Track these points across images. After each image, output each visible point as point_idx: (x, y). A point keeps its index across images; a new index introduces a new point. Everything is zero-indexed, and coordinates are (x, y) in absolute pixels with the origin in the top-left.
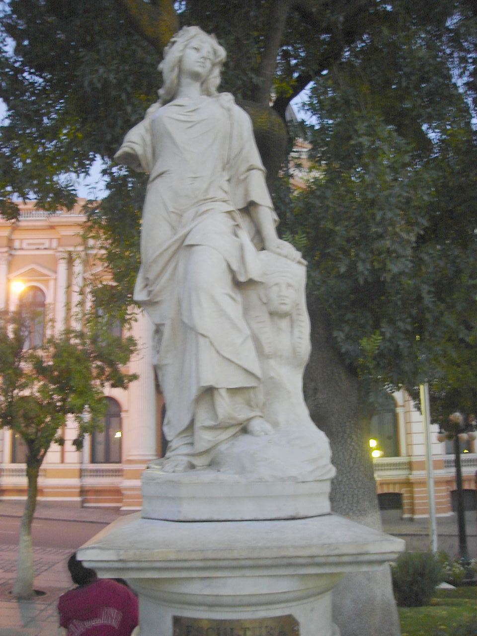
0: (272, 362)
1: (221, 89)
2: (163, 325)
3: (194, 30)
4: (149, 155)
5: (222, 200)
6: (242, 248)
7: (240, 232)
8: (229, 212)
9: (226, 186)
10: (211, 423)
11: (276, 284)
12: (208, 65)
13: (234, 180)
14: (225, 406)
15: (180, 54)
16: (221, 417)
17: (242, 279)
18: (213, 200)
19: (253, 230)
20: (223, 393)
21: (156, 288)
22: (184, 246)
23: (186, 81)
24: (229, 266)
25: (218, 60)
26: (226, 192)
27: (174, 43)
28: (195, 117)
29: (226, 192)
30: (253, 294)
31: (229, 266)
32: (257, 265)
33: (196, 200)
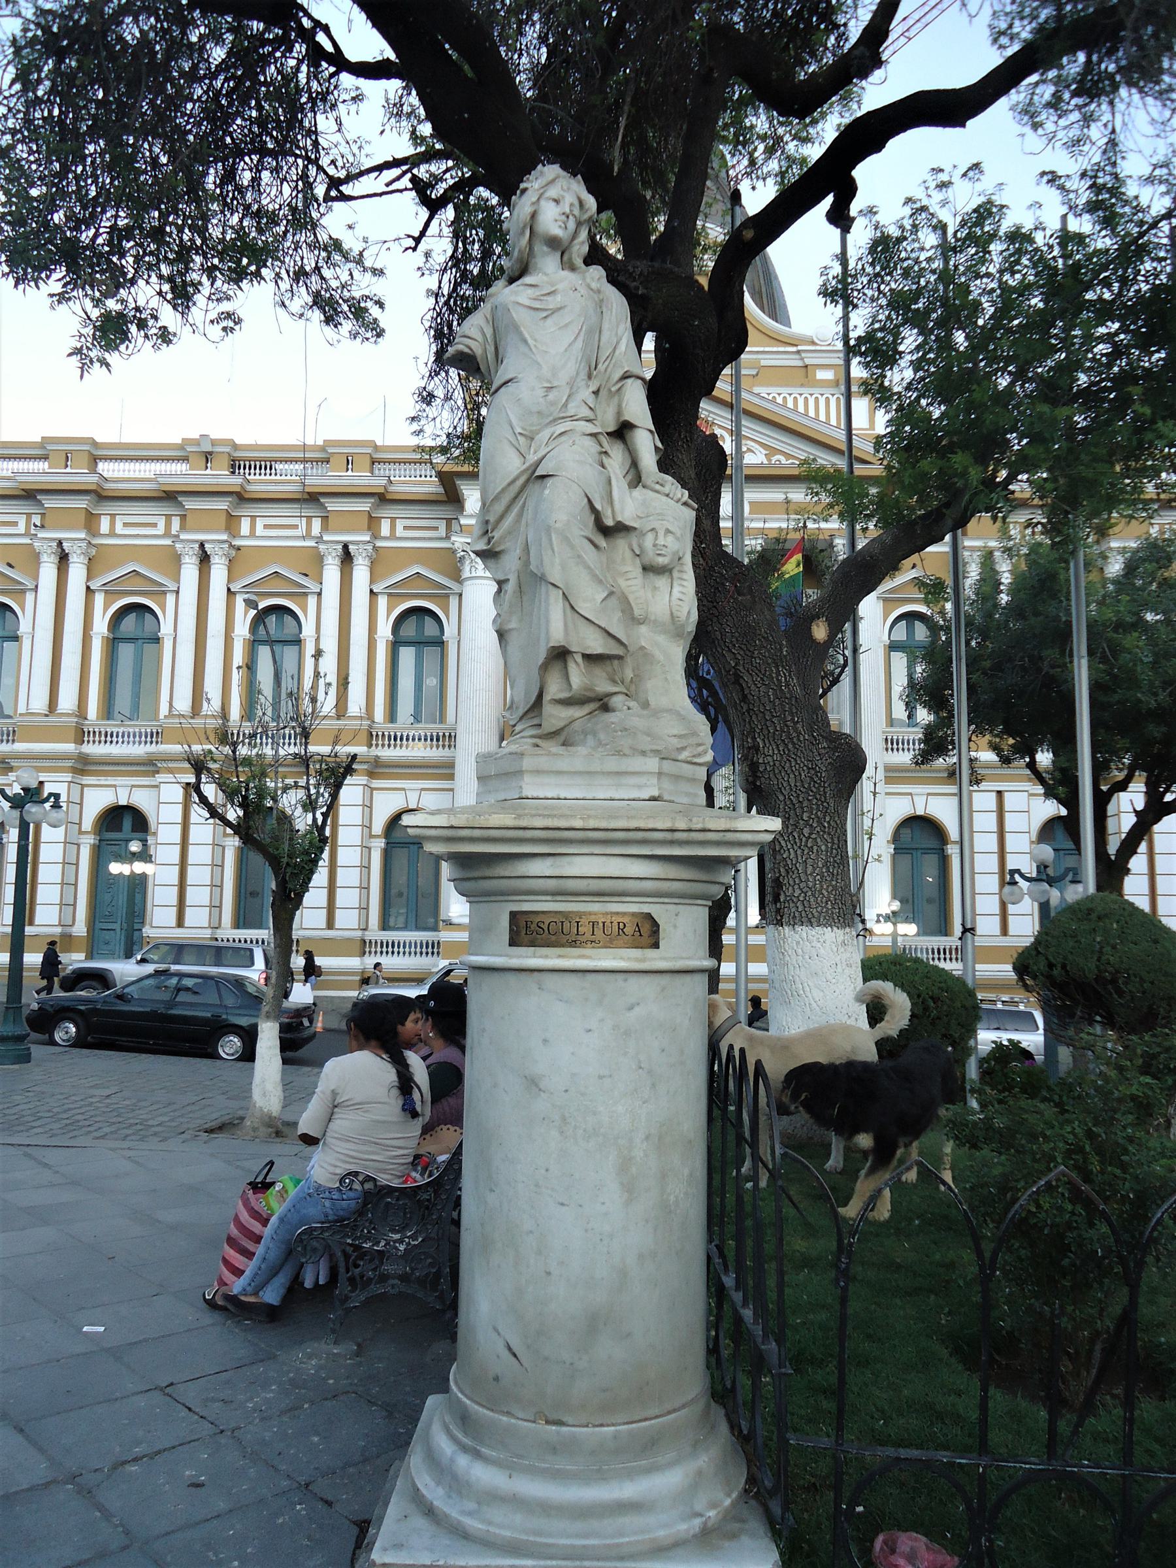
0: (643, 629)
1: (588, 262)
2: (508, 580)
3: (551, 171)
4: (491, 356)
7: (606, 460)
8: (594, 435)
9: (591, 401)
10: (564, 695)
11: (653, 529)
12: (572, 225)
13: (603, 393)
14: (578, 676)
16: (575, 686)
17: (609, 522)
18: (573, 418)
19: (630, 462)
20: (579, 659)
21: (497, 534)
22: (536, 477)
23: (540, 248)
24: (589, 501)
25: (586, 216)
27: (524, 191)
28: (552, 303)
30: (621, 544)
31: (589, 501)
32: (627, 506)
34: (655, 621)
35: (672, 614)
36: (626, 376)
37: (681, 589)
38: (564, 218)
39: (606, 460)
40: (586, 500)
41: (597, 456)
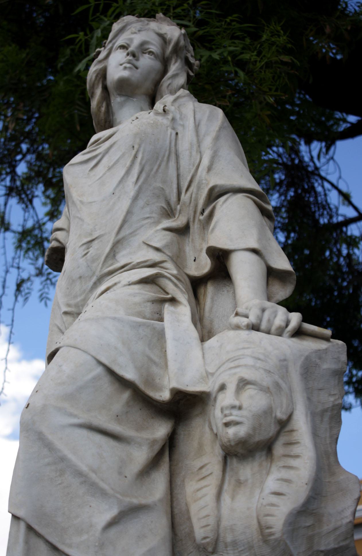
5: (148, 263)
6: (161, 335)
9: (161, 239)
12: (146, 62)
13: (195, 228)
15: (100, 66)
17: (165, 396)
26: (157, 249)
29: (157, 249)
33: (94, 279)
34: (235, 543)
35: (259, 522)
36: (215, 195)
37: (285, 474)
38: (130, 58)
39: (167, 308)
40: (100, 370)
41: (148, 309)
